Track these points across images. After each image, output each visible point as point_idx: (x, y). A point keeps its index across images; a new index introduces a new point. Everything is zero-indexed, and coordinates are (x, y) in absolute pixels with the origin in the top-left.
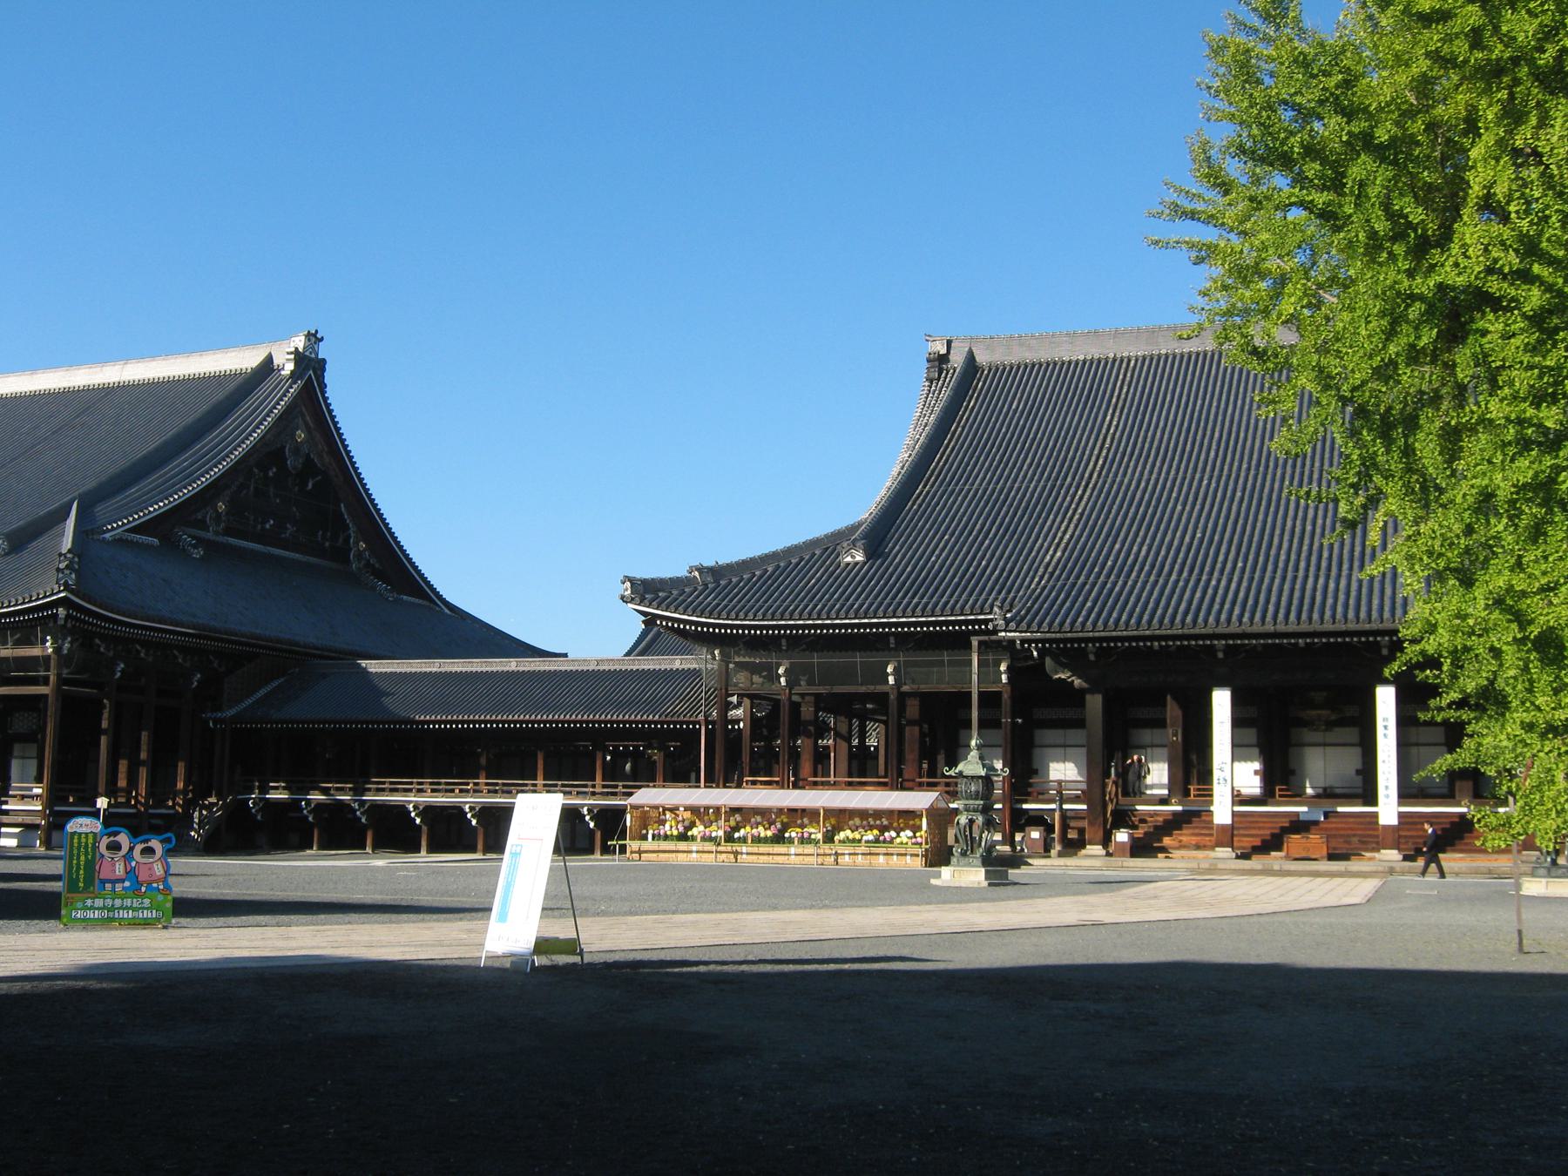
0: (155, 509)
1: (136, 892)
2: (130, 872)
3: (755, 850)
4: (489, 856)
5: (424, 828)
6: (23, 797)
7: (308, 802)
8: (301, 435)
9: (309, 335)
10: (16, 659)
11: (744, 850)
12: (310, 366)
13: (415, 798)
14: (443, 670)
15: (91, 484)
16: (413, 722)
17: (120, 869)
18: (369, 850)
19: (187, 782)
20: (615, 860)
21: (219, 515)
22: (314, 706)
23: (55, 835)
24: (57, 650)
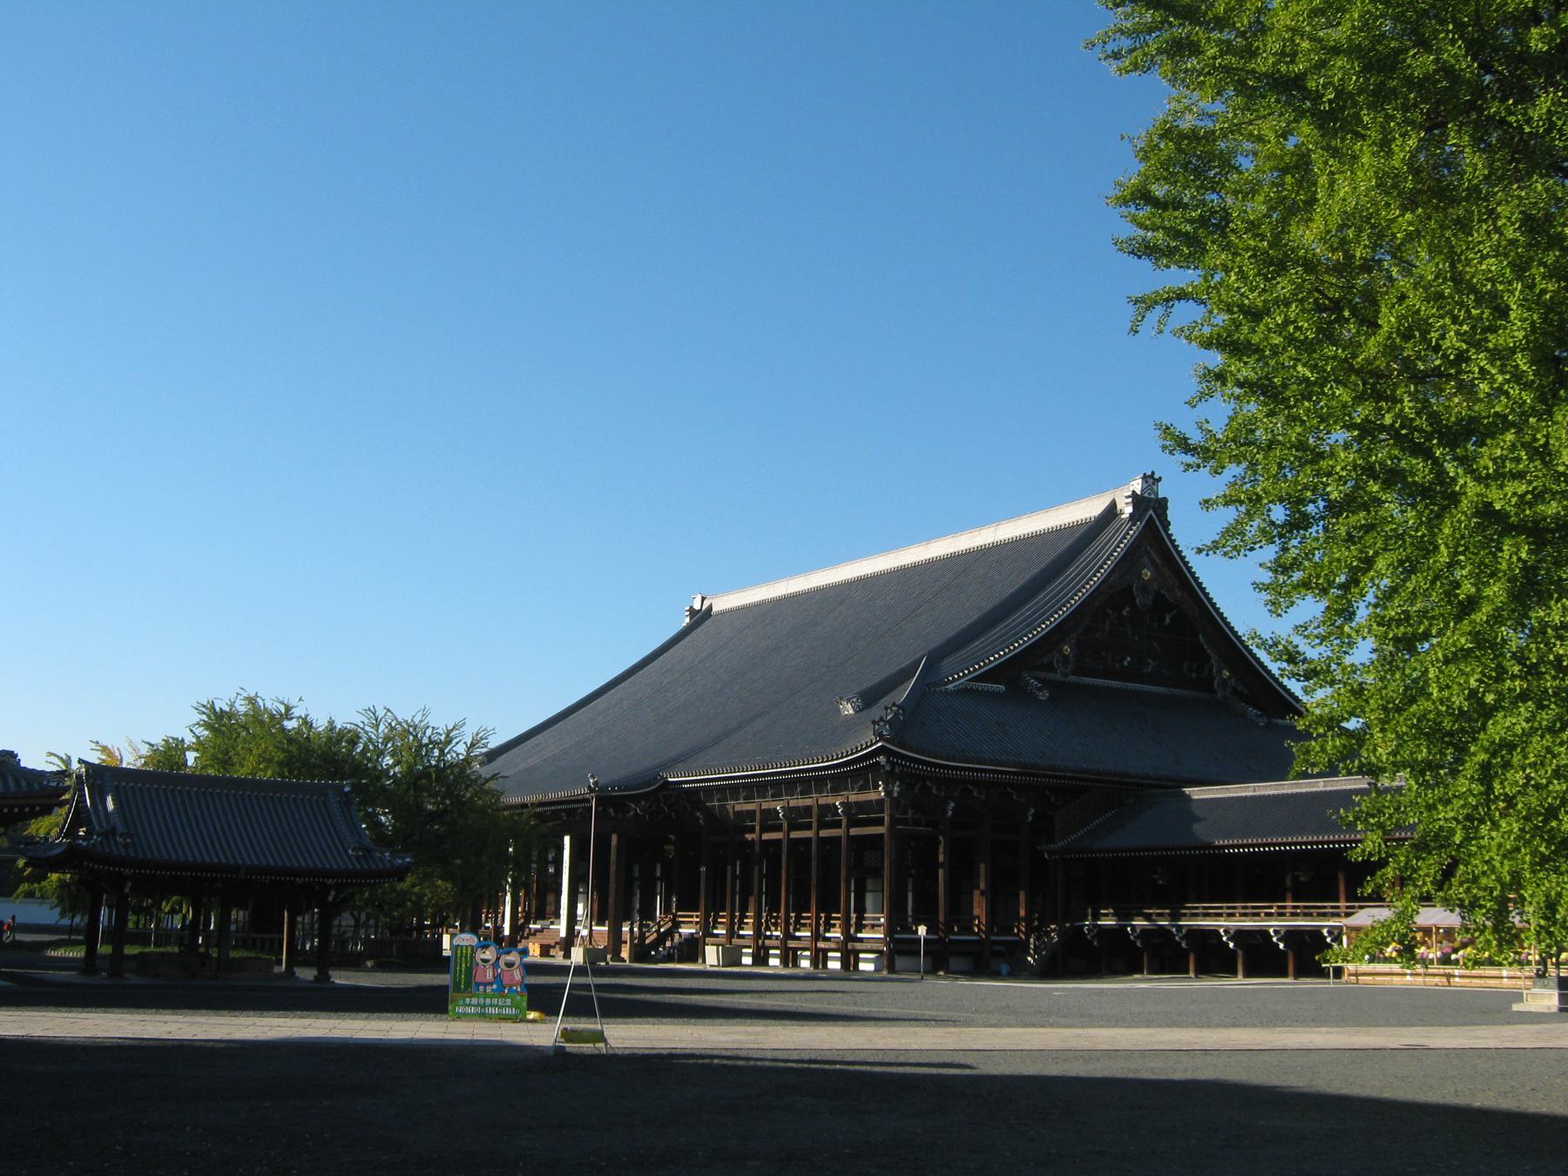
0: (995, 659)
1: (500, 993)
2: (497, 978)
3: (1467, 972)
4: (1302, 980)
5: (1240, 952)
6: (873, 926)
7: (1133, 927)
8: (1147, 574)
9: (1145, 477)
10: (857, 803)
11: (1457, 972)
12: (1151, 507)
13: (1226, 922)
14: (1257, 793)
15: (938, 639)
16: (1211, 847)
17: (489, 975)
18: (1192, 975)
19: (1029, 911)
20: (1331, 983)
21: (1066, 658)
22: (1138, 834)
23: (900, 962)
24: (889, 793)
